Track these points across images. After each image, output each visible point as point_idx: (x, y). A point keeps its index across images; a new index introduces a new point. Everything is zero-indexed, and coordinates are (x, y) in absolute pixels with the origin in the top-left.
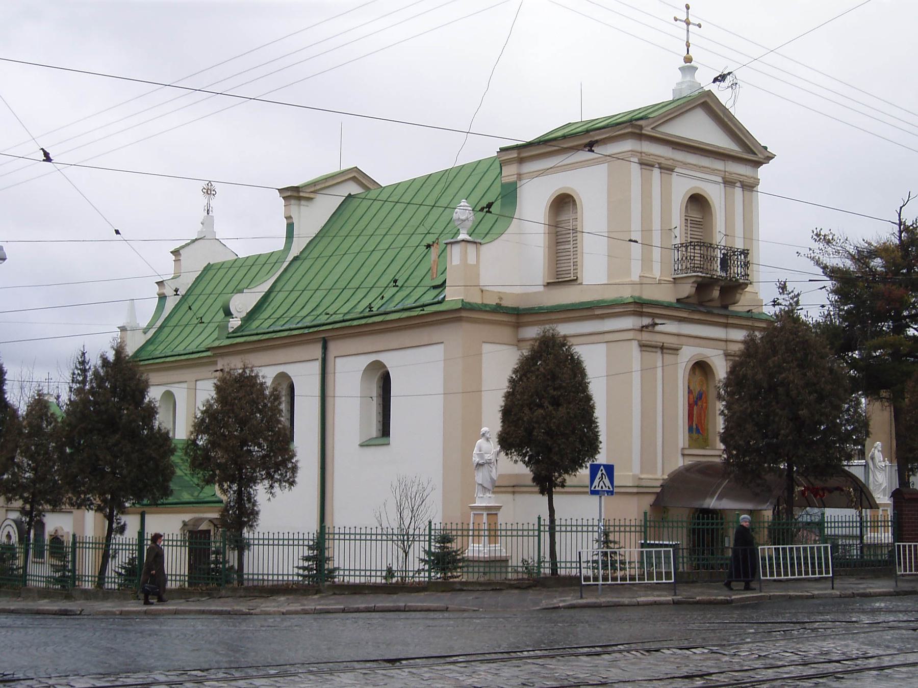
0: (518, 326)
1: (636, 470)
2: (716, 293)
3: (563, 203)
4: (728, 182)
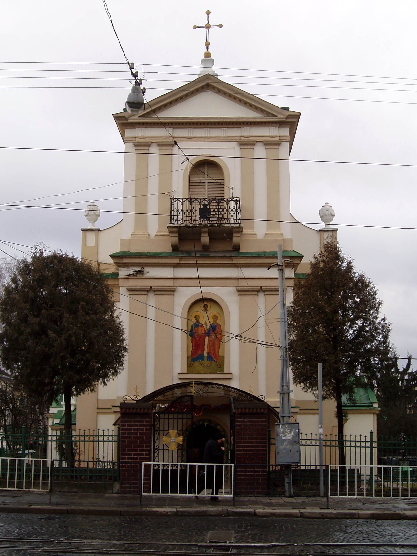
4: (246, 144)
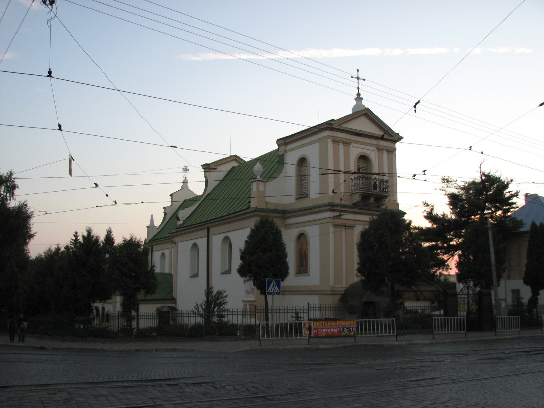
0: (285, 218)
1: (332, 283)
2: (372, 200)
3: (302, 161)
4: (380, 149)
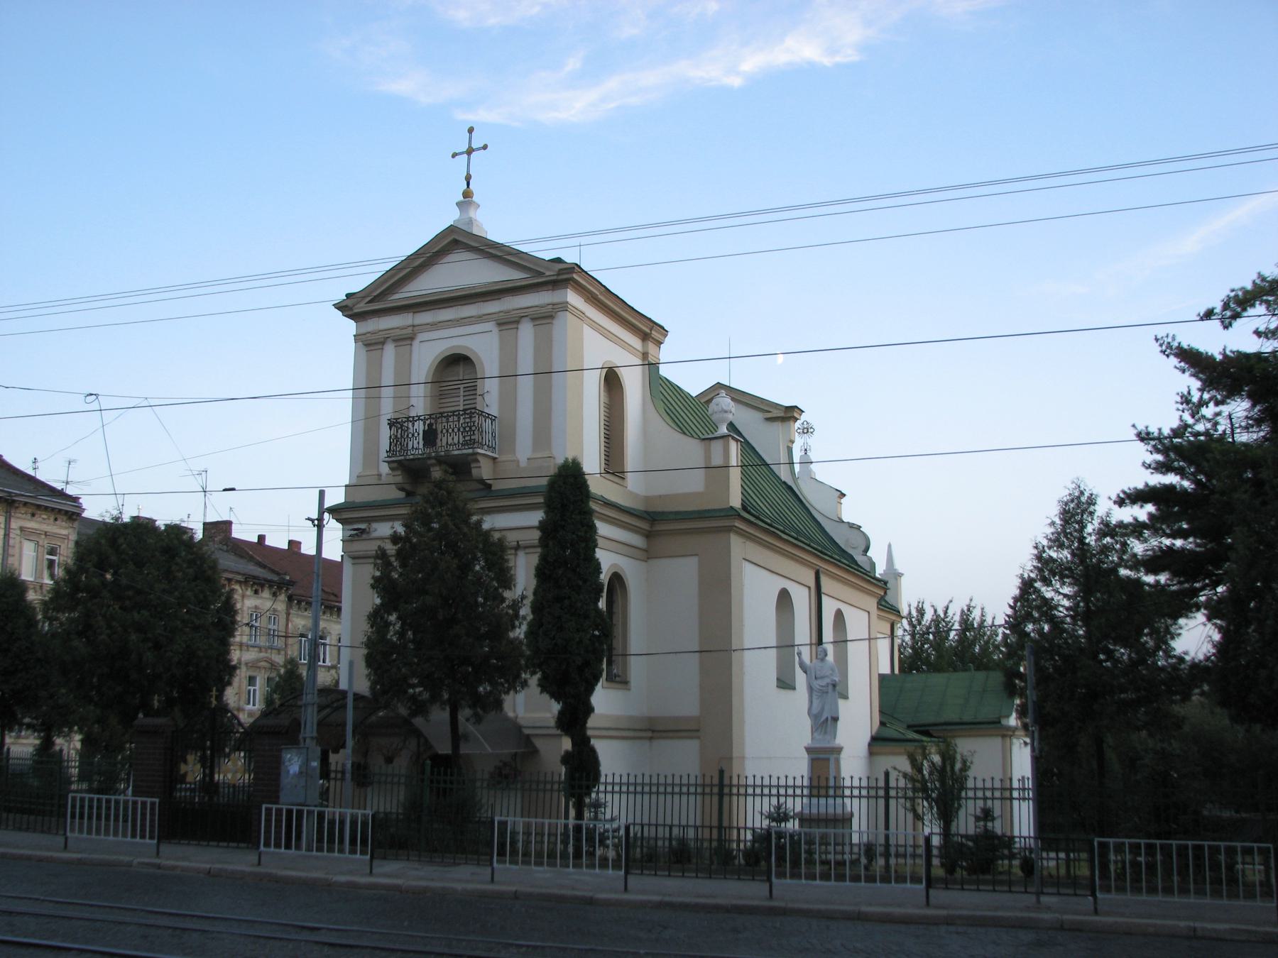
4: (508, 323)
